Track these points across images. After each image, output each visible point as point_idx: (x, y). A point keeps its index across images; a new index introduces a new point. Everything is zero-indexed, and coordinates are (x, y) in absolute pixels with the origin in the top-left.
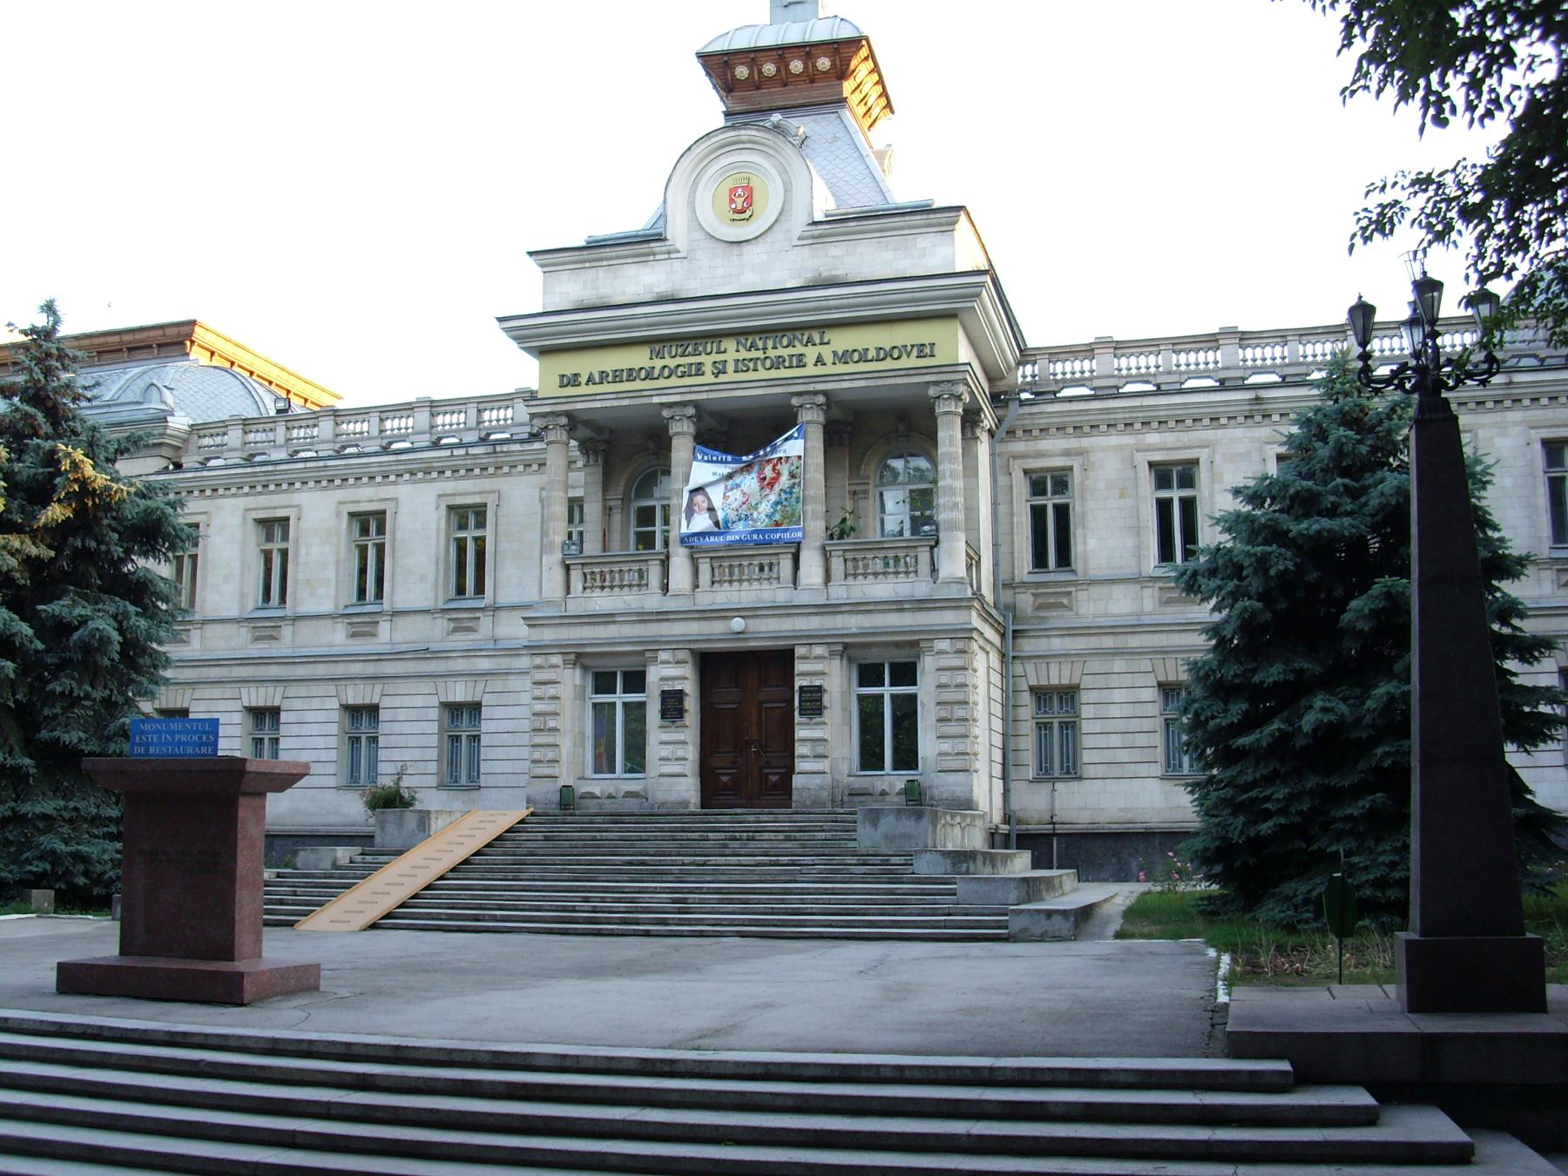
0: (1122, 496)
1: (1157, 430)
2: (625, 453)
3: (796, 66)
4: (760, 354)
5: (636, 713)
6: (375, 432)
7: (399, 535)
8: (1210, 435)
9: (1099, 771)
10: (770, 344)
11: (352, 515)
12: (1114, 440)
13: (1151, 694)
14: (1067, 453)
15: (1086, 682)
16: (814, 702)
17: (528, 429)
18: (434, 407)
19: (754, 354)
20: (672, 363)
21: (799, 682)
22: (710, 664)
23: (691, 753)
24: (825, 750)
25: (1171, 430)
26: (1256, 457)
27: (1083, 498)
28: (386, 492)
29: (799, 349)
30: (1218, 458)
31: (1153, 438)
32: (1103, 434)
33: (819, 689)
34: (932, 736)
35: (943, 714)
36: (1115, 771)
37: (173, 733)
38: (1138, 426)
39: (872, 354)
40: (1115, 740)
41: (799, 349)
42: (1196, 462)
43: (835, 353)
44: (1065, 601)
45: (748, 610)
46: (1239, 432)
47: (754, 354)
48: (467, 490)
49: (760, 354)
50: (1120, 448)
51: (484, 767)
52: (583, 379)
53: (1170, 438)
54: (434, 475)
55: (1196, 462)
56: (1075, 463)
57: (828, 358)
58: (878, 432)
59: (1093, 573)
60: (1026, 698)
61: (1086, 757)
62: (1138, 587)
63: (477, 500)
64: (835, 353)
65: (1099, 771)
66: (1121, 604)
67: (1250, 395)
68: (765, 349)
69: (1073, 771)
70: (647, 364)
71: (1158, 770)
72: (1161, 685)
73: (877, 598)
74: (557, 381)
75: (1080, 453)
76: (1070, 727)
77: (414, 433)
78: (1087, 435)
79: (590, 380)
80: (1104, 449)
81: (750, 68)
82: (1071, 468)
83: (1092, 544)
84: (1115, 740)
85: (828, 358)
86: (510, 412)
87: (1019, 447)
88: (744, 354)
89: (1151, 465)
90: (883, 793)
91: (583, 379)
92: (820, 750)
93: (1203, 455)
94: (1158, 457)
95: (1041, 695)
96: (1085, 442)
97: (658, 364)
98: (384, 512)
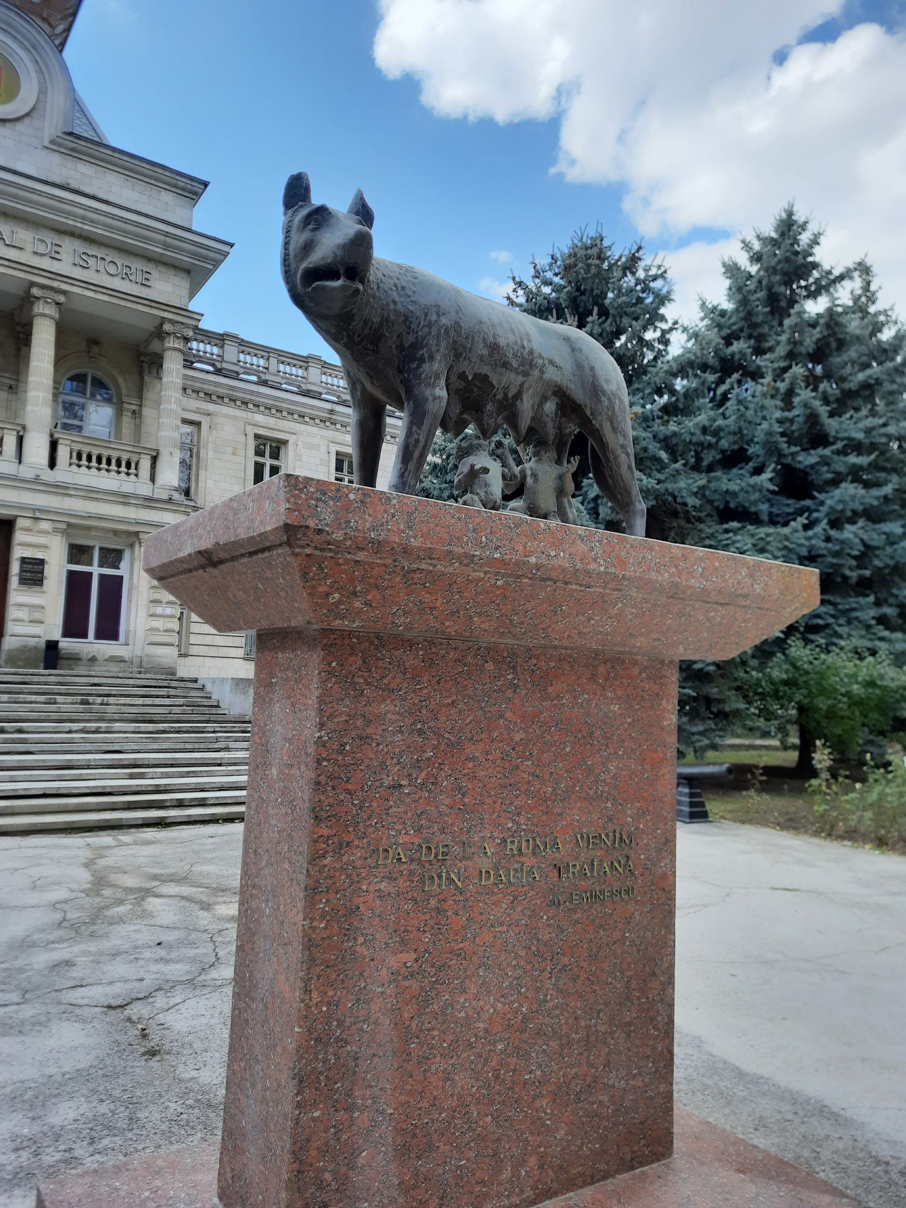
8: (297, 427)
9: (202, 650)
14: (198, 411)
16: (34, 573)
25: (273, 416)
26: (324, 449)
30: (300, 443)
31: (259, 418)
32: (226, 405)
33: (42, 562)
34: (142, 614)
36: (213, 651)
42: (285, 442)
46: (315, 430)
50: (235, 418)
53: (271, 421)
55: (285, 442)
65: (202, 650)
67: (329, 406)
71: (240, 653)
73: (100, 496)
80: (226, 416)
83: (210, 483)
89: (257, 436)
90: (93, 660)
92: (37, 616)
93: (292, 439)
96: (211, 407)
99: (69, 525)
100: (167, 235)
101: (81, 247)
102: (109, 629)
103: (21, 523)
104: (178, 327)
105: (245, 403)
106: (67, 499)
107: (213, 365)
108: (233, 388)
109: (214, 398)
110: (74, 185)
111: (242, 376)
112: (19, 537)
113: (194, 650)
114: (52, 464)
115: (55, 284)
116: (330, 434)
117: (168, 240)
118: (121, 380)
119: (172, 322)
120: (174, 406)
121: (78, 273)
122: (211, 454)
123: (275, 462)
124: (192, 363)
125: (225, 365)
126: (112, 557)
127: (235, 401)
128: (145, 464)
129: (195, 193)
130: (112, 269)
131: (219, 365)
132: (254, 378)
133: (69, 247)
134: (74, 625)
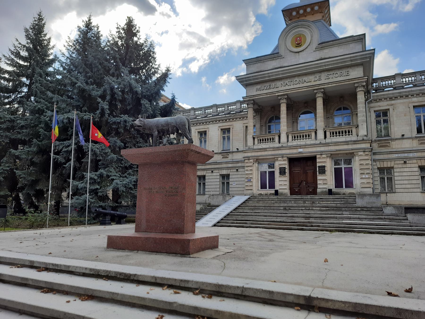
1: (416, 97)
2: (266, 113)
5: (272, 174)
6: (203, 113)
7: (209, 136)
9: (402, 190)
11: (198, 132)
13: (417, 169)
14: (388, 105)
15: (396, 166)
16: (323, 170)
17: (240, 110)
18: (217, 106)
23: (288, 183)
24: (326, 181)
28: (208, 126)
31: (415, 99)
32: (399, 99)
33: (324, 166)
35: (362, 172)
38: (410, 96)
40: (406, 182)
44: (388, 145)
45: (303, 148)
48: (225, 125)
51: (230, 189)
54: (218, 122)
58: (340, 101)
60: (376, 171)
61: (397, 186)
62: (411, 140)
63: (228, 127)
65: (402, 190)
69: (392, 191)
72: (419, 167)
76: (390, 180)
78: (394, 100)
82: (389, 109)
83: (396, 129)
84: (406, 182)
86: (235, 107)
87: (372, 105)
90: (344, 194)
92: (325, 182)
95: (381, 170)
96: (393, 102)
98: (206, 131)
99: (331, 154)
100: (351, 57)
101: (326, 73)
102: (349, 184)
103: (318, 156)
104: (360, 83)
105: (407, 96)
106: (330, 147)
107: (392, 87)
108: (400, 93)
109: (393, 98)
110: (323, 57)
111: (405, 87)
112: (318, 160)
113: (397, 190)
114: (325, 137)
115: (320, 87)
117: (352, 59)
118: (351, 106)
119: (357, 83)
120: (361, 109)
121: (327, 81)
122: (395, 119)
123: (385, 118)
124: (383, 90)
125: (396, 86)
126: (349, 162)
127: (413, 95)
128: (313, 134)
129: (362, 39)
130: (337, 76)
131: (394, 86)
132: (412, 85)
133: (324, 75)
134: (338, 184)
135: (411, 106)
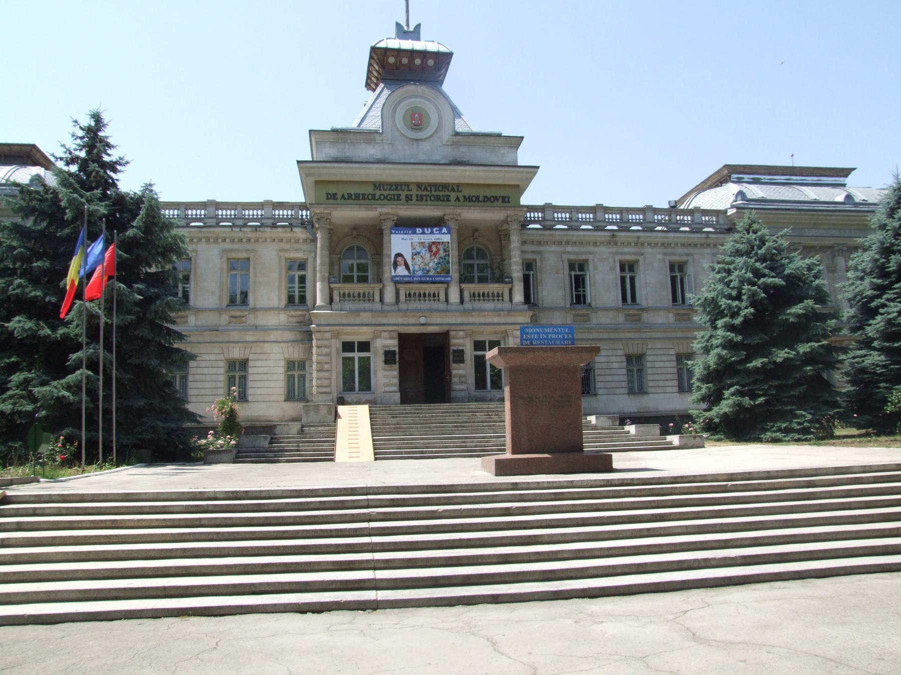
0: (557, 273)
3: (418, 62)
4: (428, 193)
8: (592, 249)
10: (433, 189)
12: (553, 248)
19: (425, 193)
20: (386, 193)
21: (452, 348)
22: (403, 338)
27: (541, 273)
29: (447, 193)
30: (596, 260)
37: (547, 334)
39: (481, 198)
41: (447, 193)
42: (587, 261)
43: (464, 196)
47: (425, 193)
49: (428, 193)
52: (339, 196)
53: (576, 249)
56: (538, 258)
57: (461, 199)
59: (545, 305)
64: (464, 196)
66: (605, 318)
68: (431, 191)
70: (373, 192)
74: (325, 197)
75: (539, 253)
77: (235, 218)
79: (343, 197)
81: (396, 59)
82: (535, 260)
83: (545, 293)
85: (461, 199)
88: (420, 193)
91: (339, 196)
93: (590, 257)
94: (572, 257)
96: (542, 249)
97: (378, 193)
116: (614, 250)
135: (566, 257)
